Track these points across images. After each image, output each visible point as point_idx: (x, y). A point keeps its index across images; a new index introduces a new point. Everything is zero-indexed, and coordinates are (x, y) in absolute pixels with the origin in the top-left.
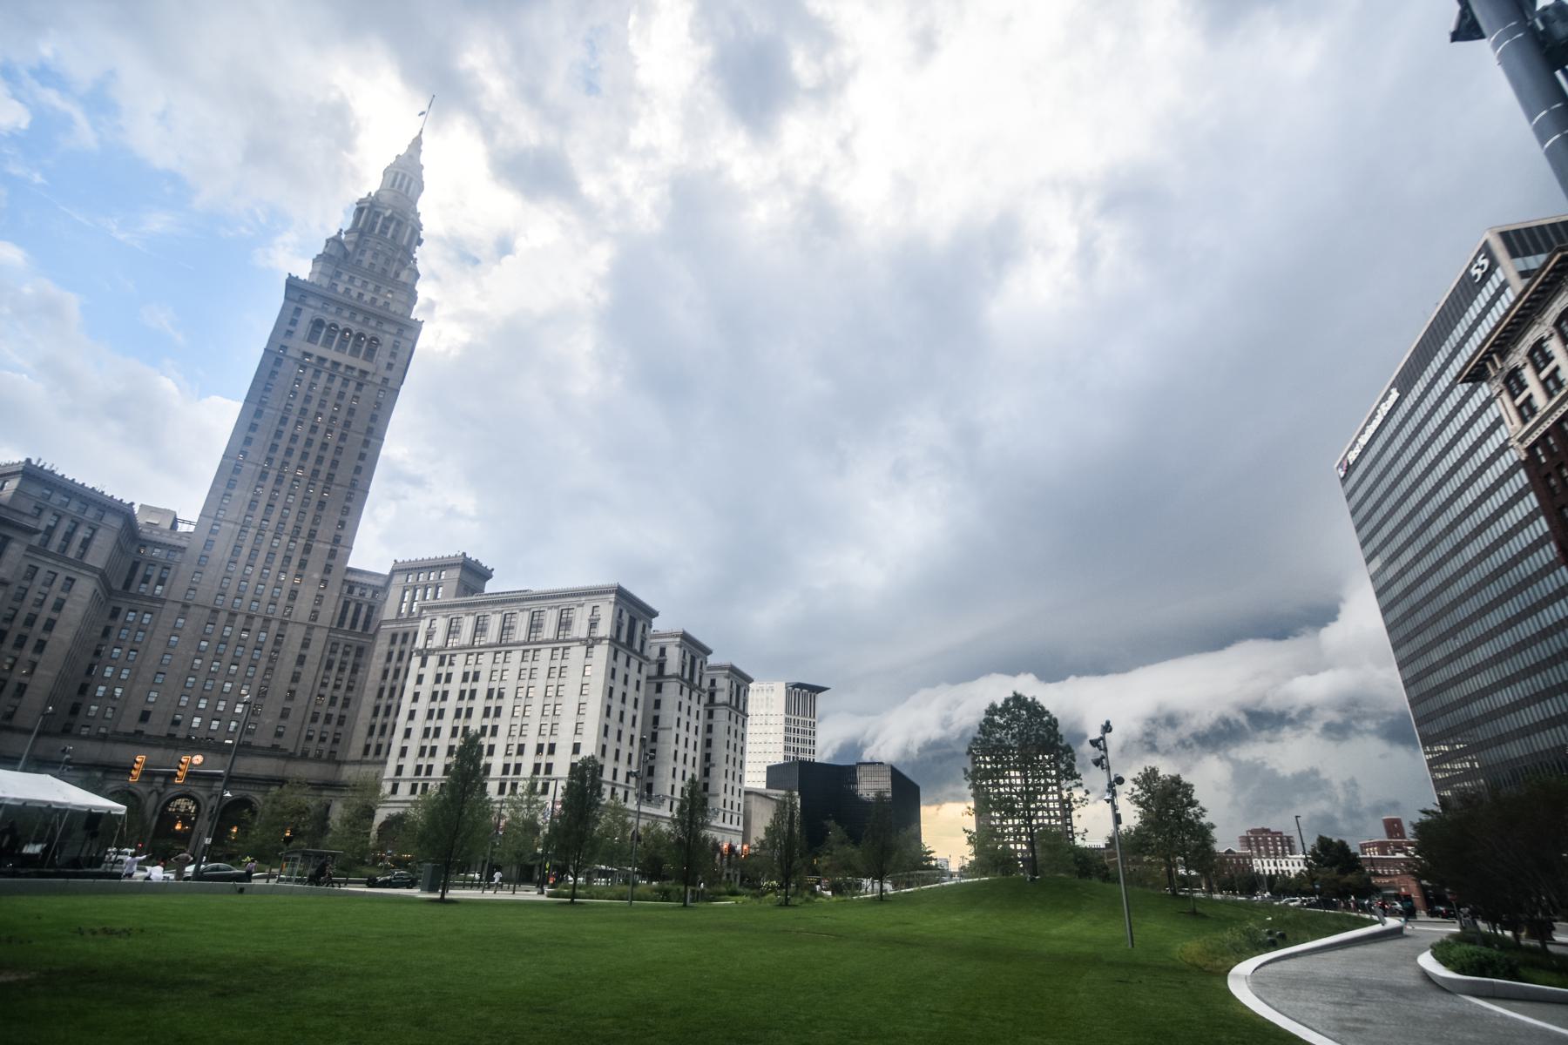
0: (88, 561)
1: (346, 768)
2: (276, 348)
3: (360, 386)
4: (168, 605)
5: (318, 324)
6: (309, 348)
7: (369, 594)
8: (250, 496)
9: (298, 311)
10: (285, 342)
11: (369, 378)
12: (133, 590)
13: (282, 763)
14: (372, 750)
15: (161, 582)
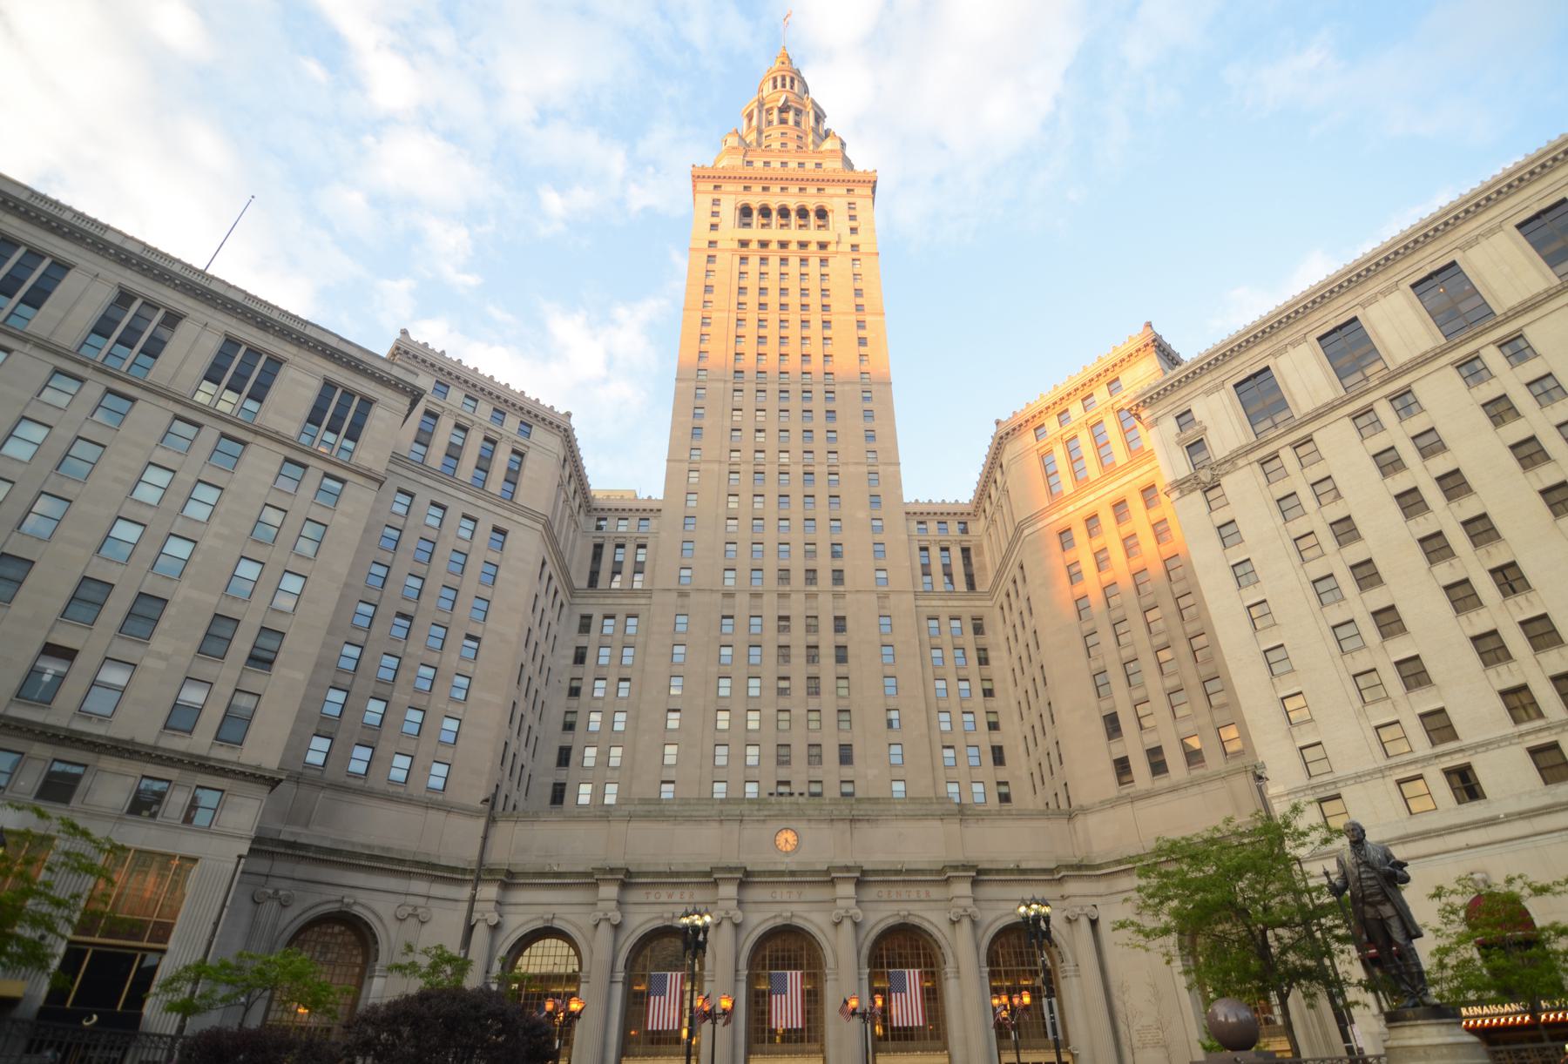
0: (522, 497)
1: (1093, 821)
2: (706, 244)
3: (824, 261)
4: (656, 597)
5: (746, 211)
6: (745, 234)
7: (954, 527)
8: (728, 424)
9: (716, 202)
10: (713, 236)
11: (831, 248)
12: (602, 584)
13: (954, 826)
14: (1140, 766)
15: (639, 568)
